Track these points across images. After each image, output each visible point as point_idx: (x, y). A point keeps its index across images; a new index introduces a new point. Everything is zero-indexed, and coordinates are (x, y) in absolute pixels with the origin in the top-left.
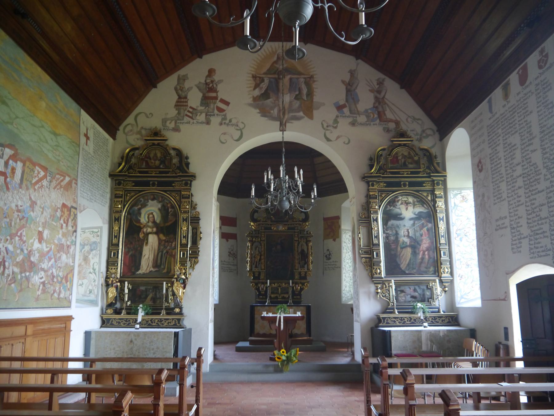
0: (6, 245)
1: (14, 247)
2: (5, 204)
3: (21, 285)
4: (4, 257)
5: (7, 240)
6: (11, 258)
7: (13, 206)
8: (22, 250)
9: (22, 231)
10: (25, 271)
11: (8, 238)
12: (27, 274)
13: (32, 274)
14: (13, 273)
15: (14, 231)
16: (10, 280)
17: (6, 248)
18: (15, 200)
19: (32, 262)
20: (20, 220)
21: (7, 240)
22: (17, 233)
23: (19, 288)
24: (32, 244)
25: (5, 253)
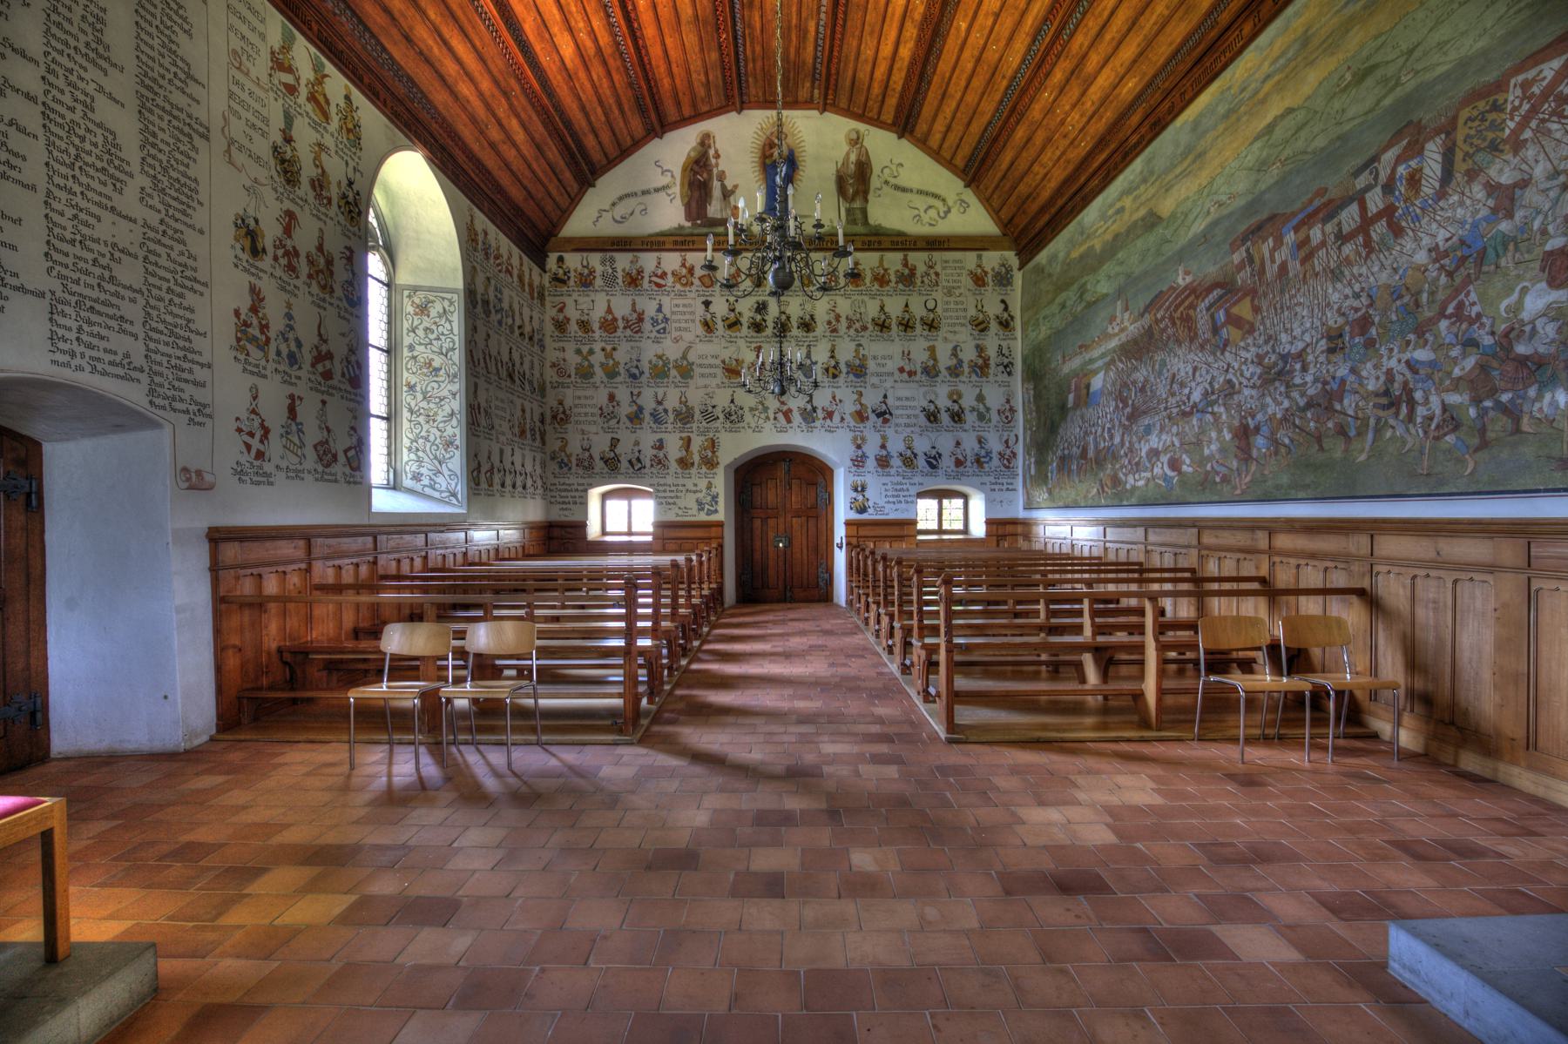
0: (1407, 356)
1: (1439, 347)
2: (1395, 270)
3: (1483, 431)
4: (1406, 383)
5: (1408, 343)
6: (1429, 377)
7: (1421, 257)
8: (1470, 343)
9: (1462, 296)
10: (1493, 392)
11: (1412, 337)
12: (1505, 397)
13: (1532, 392)
14: (1445, 408)
15: (1428, 314)
16: (1438, 427)
17: (1407, 362)
18: (1426, 241)
19: (1522, 361)
20: (1450, 274)
21: (1408, 343)
22: (1444, 308)
23: (1476, 441)
24: (1518, 307)
25: (1409, 375)
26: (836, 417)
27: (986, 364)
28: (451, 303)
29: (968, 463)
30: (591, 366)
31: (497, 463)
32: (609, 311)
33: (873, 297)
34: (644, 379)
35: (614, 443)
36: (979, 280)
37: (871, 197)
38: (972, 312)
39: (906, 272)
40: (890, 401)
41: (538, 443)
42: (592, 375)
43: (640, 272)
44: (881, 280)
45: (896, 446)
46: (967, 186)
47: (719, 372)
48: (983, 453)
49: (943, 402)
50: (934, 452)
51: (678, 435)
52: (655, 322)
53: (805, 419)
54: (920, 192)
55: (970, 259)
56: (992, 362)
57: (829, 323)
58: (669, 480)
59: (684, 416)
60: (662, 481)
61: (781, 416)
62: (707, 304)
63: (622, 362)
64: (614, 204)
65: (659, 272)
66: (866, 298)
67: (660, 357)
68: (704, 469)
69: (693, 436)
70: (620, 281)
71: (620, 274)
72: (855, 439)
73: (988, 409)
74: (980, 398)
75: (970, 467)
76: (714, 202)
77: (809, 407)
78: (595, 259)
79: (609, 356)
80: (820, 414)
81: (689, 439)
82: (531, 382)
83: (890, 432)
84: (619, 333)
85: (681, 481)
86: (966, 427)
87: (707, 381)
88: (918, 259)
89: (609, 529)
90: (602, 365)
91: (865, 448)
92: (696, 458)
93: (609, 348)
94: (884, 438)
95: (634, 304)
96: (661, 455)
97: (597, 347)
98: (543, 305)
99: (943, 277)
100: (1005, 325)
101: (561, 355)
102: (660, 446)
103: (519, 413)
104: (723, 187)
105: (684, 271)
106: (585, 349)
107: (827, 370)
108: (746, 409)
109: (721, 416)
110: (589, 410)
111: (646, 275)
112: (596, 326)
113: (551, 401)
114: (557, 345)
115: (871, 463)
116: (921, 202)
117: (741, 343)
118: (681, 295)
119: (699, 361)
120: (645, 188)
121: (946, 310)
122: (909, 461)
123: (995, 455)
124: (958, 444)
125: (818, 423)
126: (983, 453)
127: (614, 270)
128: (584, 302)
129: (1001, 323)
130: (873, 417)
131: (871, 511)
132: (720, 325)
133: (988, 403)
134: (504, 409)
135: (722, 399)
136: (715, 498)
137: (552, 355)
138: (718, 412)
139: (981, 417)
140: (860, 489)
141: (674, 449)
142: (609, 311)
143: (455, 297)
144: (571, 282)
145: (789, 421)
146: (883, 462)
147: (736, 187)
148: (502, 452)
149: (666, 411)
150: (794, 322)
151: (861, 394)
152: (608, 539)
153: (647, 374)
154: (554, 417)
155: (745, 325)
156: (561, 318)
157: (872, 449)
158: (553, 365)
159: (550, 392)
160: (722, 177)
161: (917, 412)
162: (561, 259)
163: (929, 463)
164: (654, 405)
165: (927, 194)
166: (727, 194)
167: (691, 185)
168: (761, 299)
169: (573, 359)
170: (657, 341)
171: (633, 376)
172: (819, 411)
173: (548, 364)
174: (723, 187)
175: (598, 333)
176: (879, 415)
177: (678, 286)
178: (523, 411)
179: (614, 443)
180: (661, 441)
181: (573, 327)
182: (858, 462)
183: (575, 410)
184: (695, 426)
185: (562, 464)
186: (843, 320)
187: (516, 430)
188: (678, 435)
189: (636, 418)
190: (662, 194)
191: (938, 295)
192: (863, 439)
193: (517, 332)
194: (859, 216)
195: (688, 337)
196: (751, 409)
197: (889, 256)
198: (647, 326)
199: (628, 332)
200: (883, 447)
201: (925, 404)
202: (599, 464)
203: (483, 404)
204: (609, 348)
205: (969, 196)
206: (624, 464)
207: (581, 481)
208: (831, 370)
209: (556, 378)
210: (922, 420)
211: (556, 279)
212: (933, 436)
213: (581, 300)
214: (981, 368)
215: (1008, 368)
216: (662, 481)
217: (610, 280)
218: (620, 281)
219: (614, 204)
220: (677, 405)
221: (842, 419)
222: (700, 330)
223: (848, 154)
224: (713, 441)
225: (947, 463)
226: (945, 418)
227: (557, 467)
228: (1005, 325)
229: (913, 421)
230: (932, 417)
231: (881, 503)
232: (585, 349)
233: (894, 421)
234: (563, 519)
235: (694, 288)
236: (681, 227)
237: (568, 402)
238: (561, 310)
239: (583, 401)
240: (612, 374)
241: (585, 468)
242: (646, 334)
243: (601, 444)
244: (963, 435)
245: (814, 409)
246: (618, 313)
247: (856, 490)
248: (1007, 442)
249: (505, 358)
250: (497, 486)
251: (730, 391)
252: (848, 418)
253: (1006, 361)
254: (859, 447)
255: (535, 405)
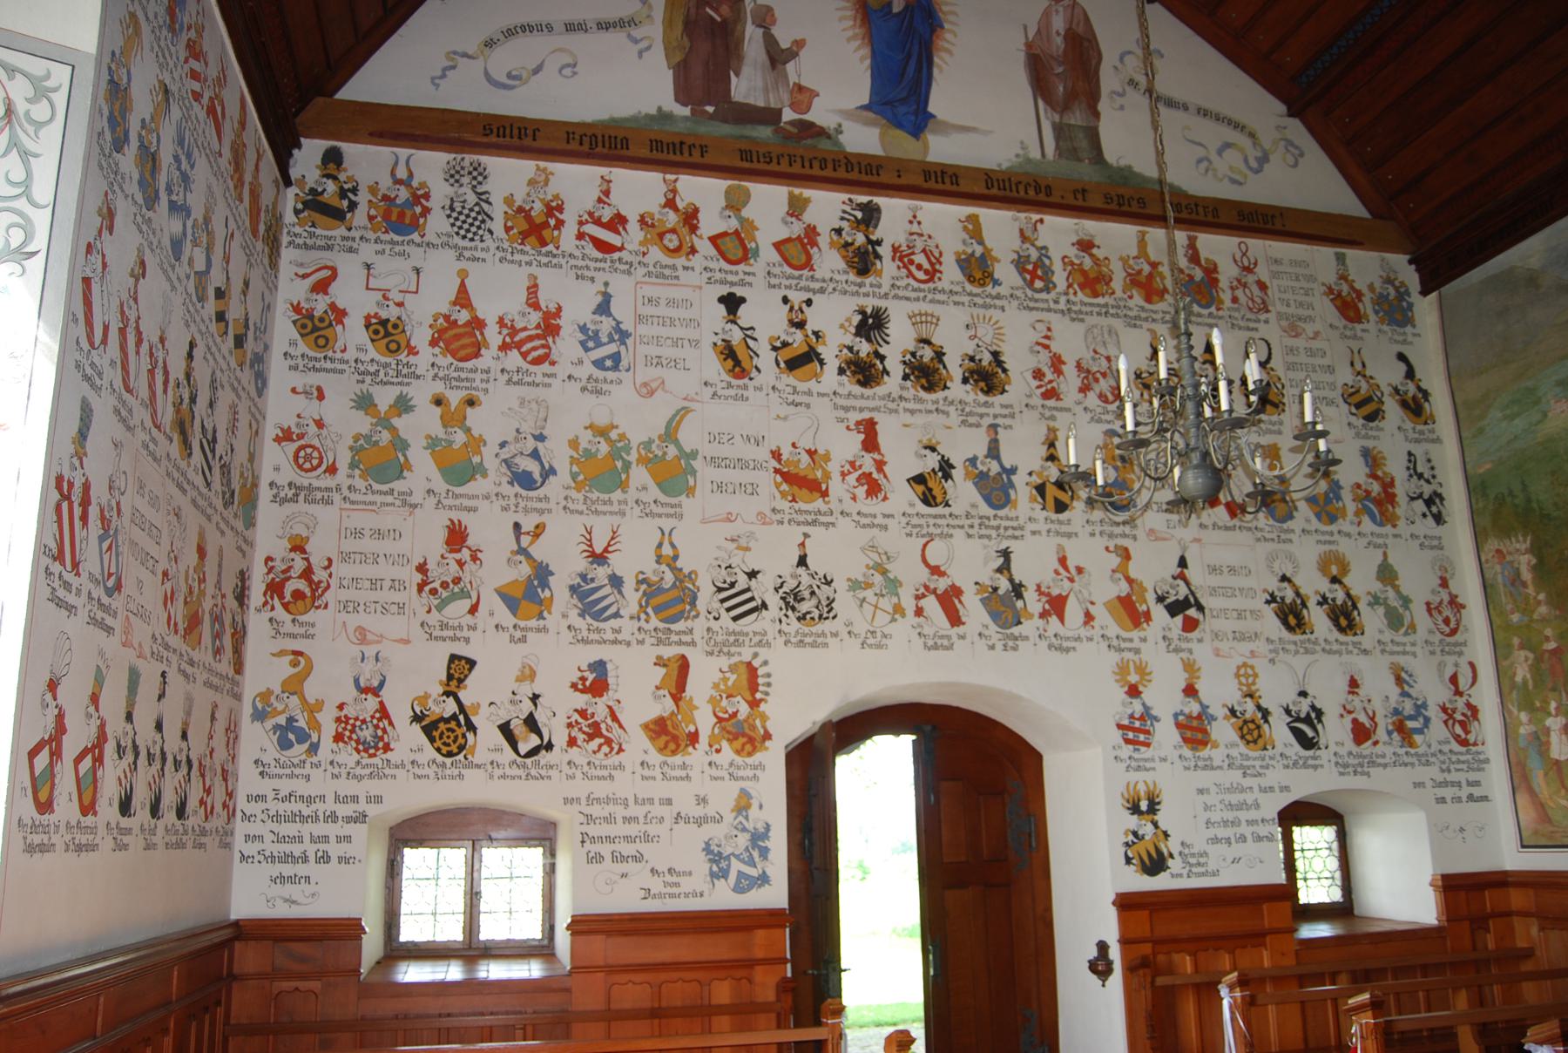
26: (1073, 611)
27: (1388, 497)
28: (41, 92)
29: (1381, 734)
30: (400, 445)
31: (116, 726)
32: (463, 298)
33: (1133, 322)
34: (554, 488)
35: (459, 669)
36: (1348, 308)
37: (1101, 107)
38: (1345, 376)
39: (1198, 274)
40: (1194, 573)
41: (225, 667)
42: (401, 469)
43: (554, 208)
44: (1147, 286)
45: (1219, 691)
46: (1291, 114)
47: (766, 480)
48: (1408, 708)
49: (1312, 583)
50: (1304, 707)
51: (651, 651)
52: (589, 338)
53: (995, 616)
54: (1203, 113)
55: (1323, 256)
56: (1401, 490)
57: (1038, 374)
58: (625, 785)
59: (670, 599)
60: (601, 789)
61: (931, 605)
62: (732, 303)
63: (493, 441)
64: (490, 44)
65: (607, 214)
66: (1117, 324)
67: (602, 432)
68: (728, 753)
69: (695, 657)
70: (497, 226)
71: (498, 210)
72: (1122, 670)
73: (1406, 601)
74: (1386, 574)
75: (1386, 745)
76: (746, 70)
77: (1004, 585)
78: (430, 165)
79: (453, 419)
80: (1033, 602)
81: (684, 666)
82: (225, 469)
83: (1202, 652)
84: (488, 358)
85: (659, 789)
86: (1367, 641)
87: (735, 503)
88: (1218, 247)
89: (409, 932)
90: (432, 443)
91: (1149, 695)
92: (704, 721)
93: (455, 398)
94: (1189, 667)
95: (533, 289)
96: (599, 709)
97: (421, 393)
98: (274, 264)
99: (1274, 286)
100: (1415, 407)
101: (312, 409)
102: (596, 682)
103: (191, 558)
104: (770, 42)
105: (672, 218)
106: (384, 398)
107: (1041, 489)
108: (840, 584)
109: (774, 601)
110: (385, 571)
111: (570, 217)
112: (420, 337)
113: (270, 532)
114: (299, 380)
115: (1166, 735)
116: (1214, 134)
117: (822, 408)
118: (661, 275)
119: (708, 450)
120: (575, 16)
121: (1290, 367)
122: (1251, 731)
123: (1433, 712)
124: (1354, 684)
125: (1029, 627)
126: (1408, 708)
127: (483, 197)
128: (393, 271)
129: (1404, 404)
130: (1159, 613)
131: (1175, 865)
132: (766, 359)
133: (1406, 584)
134: (151, 529)
135: (773, 559)
136: (758, 839)
137: (281, 407)
138: (763, 589)
139: (1395, 620)
140: (1144, 806)
141: (637, 695)
142: (463, 298)
143: (61, 74)
144: (360, 217)
145: (955, 619)
146: (1194, 732)
147: (800, 44)
148: (134, 678)
149: (616, 582)
150: (954, 367)
151: (1126, 555)
152: (413, 973)
153: (563, 476)
154: (275, 588)
155: (832, 364)
156: (320, 305)
157: (1164, 698)
158: (286, 436)
159: (269, 515)
160: (765, 18)
161: (1258, 603)
162: (333, 158)
163: (1298, 734)
164: (581, 564)
165: (1218, 118)
166: (778, 57)
167: (690, 26)
168: (870, 304)
169: (344, 424)
170: (593, 388)
171: (525, 481)
172: (1030, 595)
173: (270, 431)
174: (770, 42)
175: (426, 356)
176: (1175, 609)
177: (656, 254)
178: (201, 552)
179: (459, 669)
180: (599, 667)
181: (353, 334)
182: (1136, 731)
183: (341, 570)
184: (699, 625)
185: (288, 734)
186: (1069, 369)
187: (179, 611)
188: (651, 651)
189: (527, 597)
190: (617, 37)
191: (1271, 330)
192: (1142, 670)
193: (211, 306)
194: (1083, 143)
195: (681, 384)
196: (855, 585)
197: (1156, 235)
198: (566, 346)
199: (514, 359)
200: (1190, 691)
201: (1273, 584)
202: (408, 738)
203: (99, 493)
204: (455, 398)
205: (1297, 130)
206: (487, 737)
207: (347, 787)
208: (1051, 491)
209: (289, 474)
210: (1271, 624)
211: (314, 204)
212: (1300, 662)
213: (382, 264)
214: (1378, 503)
215: (1433, 503)
216: (601, 789)
217: (470, 221)
218: (497, 226)
219: (490, 44)
220: (650, 567)
221: (1089, 617)
222: (714, 368)
223: (1046, 14)
224: (752, 671)
225: (1335, 731)
226: (1318, 618)
227: (270, 743)
228: (1415, 407)
229: (1249, 625)
230: (1292, 616)
231: (1199, 845)
232: (384, 398)
233: (1208, 625)
234: (282, 911)
235: (697, 261)
236: (663, 116)
237: (318, 551)
238: (322, 287)
239: (368, 545)
240: (459, 468)
241: (364, 748)
242: (562, 370)
243: (415, 678)
244: (1360, 664)
245: (1017, 590)
246: (488, 310)
247: (1135, 809)
248: (1454, 680)
249: (177, 370)
250: (108, 810)
251: (796, 533)
252: (1101, 615)
253: (1427, 490)
254: (1134, 691)
255: (229, 541)
